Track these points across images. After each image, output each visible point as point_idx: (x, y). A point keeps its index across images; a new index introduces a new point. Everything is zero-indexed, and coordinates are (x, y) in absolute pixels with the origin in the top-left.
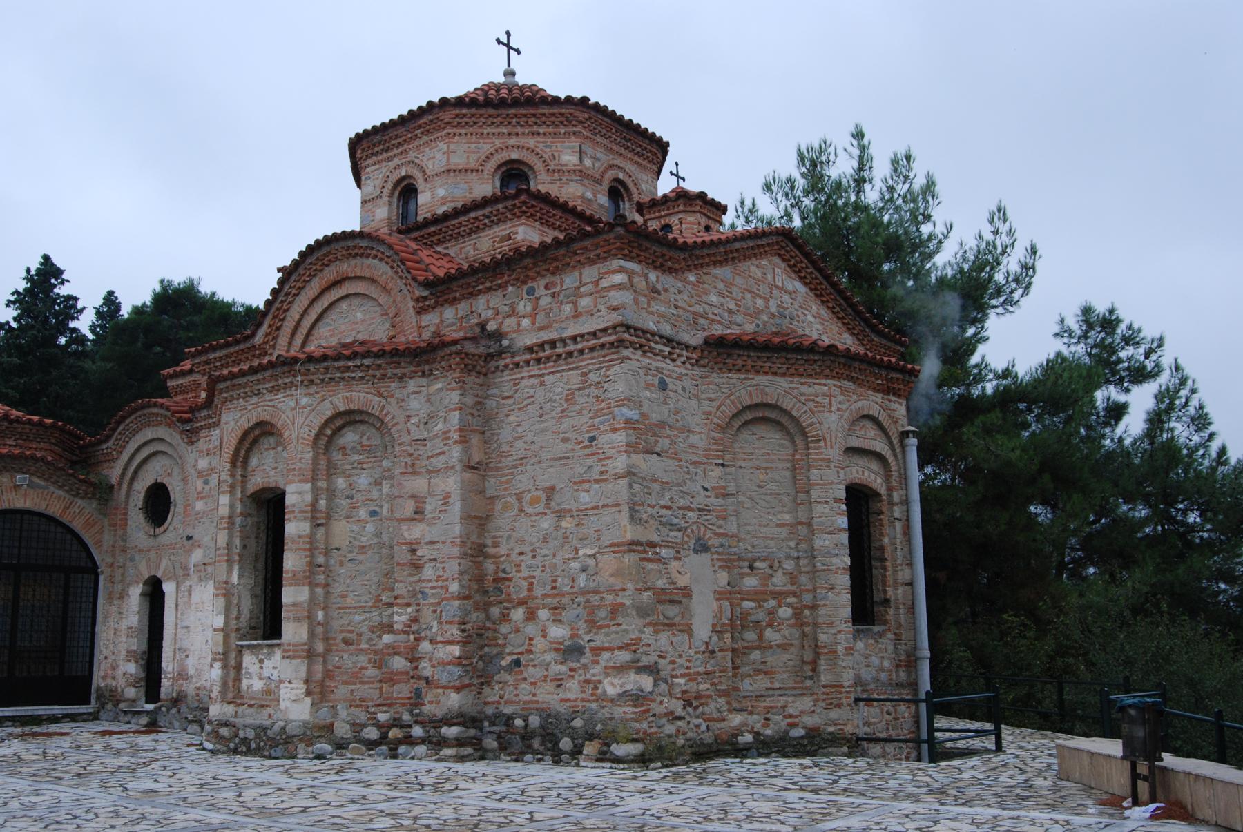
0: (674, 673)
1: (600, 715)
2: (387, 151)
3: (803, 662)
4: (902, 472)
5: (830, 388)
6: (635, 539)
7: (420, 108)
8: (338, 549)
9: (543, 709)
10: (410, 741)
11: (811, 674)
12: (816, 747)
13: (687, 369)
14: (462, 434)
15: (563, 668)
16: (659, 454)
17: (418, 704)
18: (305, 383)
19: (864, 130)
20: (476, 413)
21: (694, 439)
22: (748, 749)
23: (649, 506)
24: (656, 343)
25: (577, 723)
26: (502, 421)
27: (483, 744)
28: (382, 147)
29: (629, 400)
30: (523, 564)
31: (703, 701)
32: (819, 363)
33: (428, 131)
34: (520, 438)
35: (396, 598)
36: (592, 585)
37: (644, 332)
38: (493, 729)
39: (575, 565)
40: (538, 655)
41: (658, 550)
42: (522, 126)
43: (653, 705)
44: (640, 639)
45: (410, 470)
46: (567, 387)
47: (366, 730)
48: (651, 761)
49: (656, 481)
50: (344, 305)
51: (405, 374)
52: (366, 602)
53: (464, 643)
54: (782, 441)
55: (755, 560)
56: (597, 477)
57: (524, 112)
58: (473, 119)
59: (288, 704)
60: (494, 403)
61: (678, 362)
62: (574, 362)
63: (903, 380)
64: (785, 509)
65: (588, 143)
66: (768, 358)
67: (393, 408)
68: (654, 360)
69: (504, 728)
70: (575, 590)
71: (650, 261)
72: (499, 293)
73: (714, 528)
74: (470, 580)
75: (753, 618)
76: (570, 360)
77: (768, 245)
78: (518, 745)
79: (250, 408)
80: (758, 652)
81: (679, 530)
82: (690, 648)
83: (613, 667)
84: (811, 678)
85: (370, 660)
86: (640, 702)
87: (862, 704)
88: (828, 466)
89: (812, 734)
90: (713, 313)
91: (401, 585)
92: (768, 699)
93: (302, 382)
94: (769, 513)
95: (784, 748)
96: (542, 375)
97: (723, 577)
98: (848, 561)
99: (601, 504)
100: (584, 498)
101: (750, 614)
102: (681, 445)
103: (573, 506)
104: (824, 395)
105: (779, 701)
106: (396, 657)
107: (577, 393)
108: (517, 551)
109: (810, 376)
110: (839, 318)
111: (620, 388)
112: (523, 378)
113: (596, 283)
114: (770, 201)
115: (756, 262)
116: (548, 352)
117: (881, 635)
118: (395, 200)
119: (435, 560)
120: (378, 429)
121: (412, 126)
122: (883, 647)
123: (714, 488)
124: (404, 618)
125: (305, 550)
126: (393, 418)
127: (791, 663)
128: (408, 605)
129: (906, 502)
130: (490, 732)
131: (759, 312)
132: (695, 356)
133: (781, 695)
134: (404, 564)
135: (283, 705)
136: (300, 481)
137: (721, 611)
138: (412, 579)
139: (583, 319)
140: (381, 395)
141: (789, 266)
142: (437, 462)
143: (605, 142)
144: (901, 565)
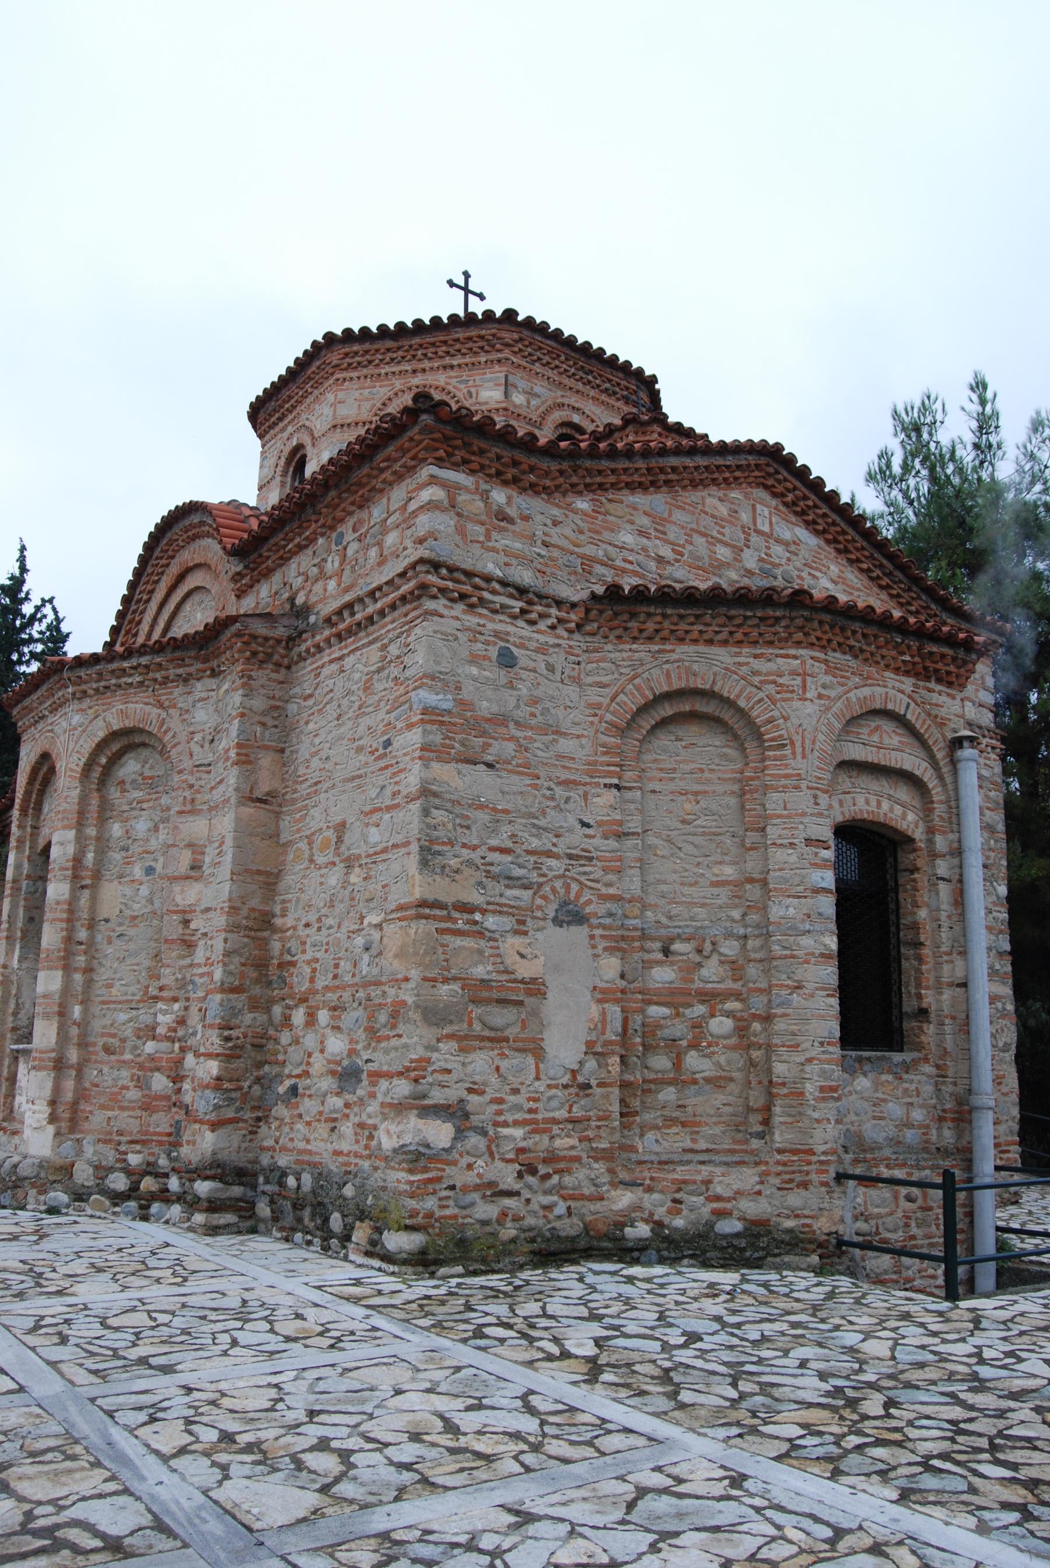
0: (501, 1118)
1: (371, 1182)
3: (749, 1109)
4: (953, 804)
5: (803, 662)
6: (430, 897)
7: (306, 352)
8: (107, 921)
10: (164, 1196)
11: (760, 1128)
12: (761, 1253)
13: (558, 637)
14: (244, 751)
15: (336, 1102)
16: (490, 766)
17: (177, 1145)
18: (78, 695)
19: (987, 380)
20: (270, 722)
21: (566, 745)
22: (642, 1250)
23: (464, 846)
24: (494, 592)
25: (349, 1191)
26: (302, 732)
27: (257, 1210)
29: (433, 678)
30: (308, 940)
31: (562, 1165)
32: (783, 624)
34: (316, 753)
35: (161, 989)
36: (375, 971)
37: (469, 574)
38: (268, 1188)
40: (316, 1080)
41: (478, 917)
42: (430, 359)
43: (449, 1170)
44: (428, 1061)
45: (189, 807)
46: (366, 670)
47: (112, 1177)
48: (439, 1263)
49: (481, 807)
51: (190, 674)
52: (134, 995)
53: (229, 1057)
54: (725, 750)
55: (672, 940)
56: (389, 803)
57: (432, 340)
58: (368, 357)
60: (295, 706)
61: (542, 625)
62: (376, 631)
63: (954, 659)
64: (727, 858)
65: (520, 373)
66: (697, 617)
67: (174, 723)
68: (493, 621)
69: (276, 1189)
70: (357, 979)
71: (493, 471)
72: (309, 551)
73: (598, 886)
74: (243, 965)
75: (666, 1033)
76: (371, 629)
77: (739, 467)
78: (289, 1220)
80: (672, 1089)
81: (526, 887)
82: (538, 1078)
83: (390, 1105)
84: (761, 1136)
85: (133, 1076)
86: (422, 1163)
87: (852, 1183)
88: (797, 788)
89: (756, 1230)
90: (625, 560)
91: (168, 970)
92: (679, 1168)
93: (74, 694)
94: (699, 864)
95: (704, 1252)
96: (341, 658)
97: (610, 967)
98: (832, 943)
99: (390, 844)
100: (375, 835)
101: (660, 1027)
102: (539, 753)
103: (361, 850)
104: (794, 673)
105: (699, 1172)
106: (156, 1074)
107: (376, 677)
108: (303, 922)
109: (770, 643)
110: (881, 587)
111: (419, 661)
112: (323, 666)
113: (404, 508)
114: (875, 494)
115: (721, 494)
117: (907, 1068)
118: (289, 479)
120: (161, 753)
122: (913, 1087)
123: (600, 824)
125: (61, 920)
126: (174, 736)
127: (728, 1109)
128: (175, 1000)
129: (958, 852)
130: (264, 1193)
131: (719, 566)
132: (573, 617)
133: (703, 1163)
134: (173, 941)
136: (64, 828)
137: (604, 1021)
138: (182, 963)
140: (161, 706)
141: (785, 504)
142: (217, 795)
143: (550, 373)
144: (950, 954)
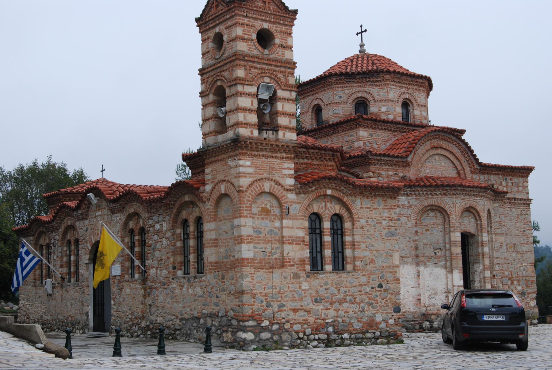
2: (399, 83)
33: (418, 85)
36: (527, 274)
39: (522, 268)
50: (437, 157)
79: (466, 200)
96: (511, 208)
100: (524, 248)
116: (513, 201)
119: (499, 264)
139: (520, 193)
142: (498, 231)
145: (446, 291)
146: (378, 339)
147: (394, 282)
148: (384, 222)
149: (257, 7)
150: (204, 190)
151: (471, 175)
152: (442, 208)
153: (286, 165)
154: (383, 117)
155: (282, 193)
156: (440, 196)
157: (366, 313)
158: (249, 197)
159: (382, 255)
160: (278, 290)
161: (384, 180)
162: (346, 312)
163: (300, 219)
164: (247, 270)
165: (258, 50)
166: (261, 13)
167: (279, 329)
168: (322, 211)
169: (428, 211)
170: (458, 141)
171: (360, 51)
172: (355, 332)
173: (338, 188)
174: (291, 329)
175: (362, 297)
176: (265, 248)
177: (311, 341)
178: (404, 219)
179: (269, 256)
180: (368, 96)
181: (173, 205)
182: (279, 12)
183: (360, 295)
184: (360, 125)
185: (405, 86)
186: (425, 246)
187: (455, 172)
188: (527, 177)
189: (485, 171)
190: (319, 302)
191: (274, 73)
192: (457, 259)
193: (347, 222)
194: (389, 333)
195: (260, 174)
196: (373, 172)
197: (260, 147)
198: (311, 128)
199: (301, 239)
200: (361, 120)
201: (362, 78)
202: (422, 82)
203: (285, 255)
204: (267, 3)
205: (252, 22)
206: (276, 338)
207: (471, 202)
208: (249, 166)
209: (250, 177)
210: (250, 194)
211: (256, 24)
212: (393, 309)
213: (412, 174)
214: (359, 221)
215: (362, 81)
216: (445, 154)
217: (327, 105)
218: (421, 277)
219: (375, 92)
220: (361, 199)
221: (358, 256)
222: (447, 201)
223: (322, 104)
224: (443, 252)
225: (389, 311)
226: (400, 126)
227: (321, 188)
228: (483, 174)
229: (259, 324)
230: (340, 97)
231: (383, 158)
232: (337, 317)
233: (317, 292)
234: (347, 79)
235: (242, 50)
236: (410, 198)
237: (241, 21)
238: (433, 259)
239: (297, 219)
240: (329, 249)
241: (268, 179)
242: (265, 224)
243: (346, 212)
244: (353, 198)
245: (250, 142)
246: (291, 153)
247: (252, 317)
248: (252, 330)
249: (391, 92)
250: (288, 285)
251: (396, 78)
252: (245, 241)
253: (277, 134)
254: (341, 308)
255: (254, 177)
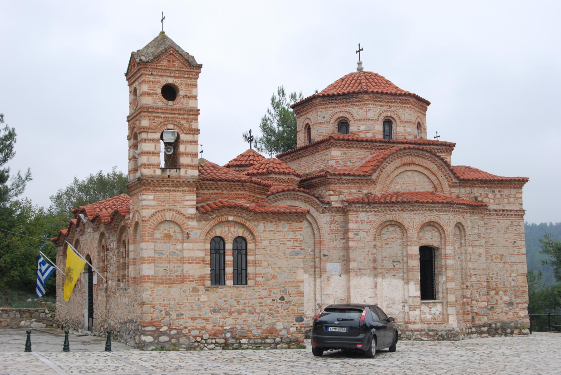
9: (502, 321)
10: (472, 333)
15: (507, 309)
28: (379, 99)
33: (402, 102)
36: (516, 285)
39: (510, 279)
50: (409, 173)
59: (453, 322)
96: (498, 219)
103: (509, 261)
108: (492, 273)
116: (501, 212)
121: (396, 98)
124: (469, 293)
135: (450, 322)
139: (511, 205)
145: (403, 301)
146: (278, 344)
147: (297, 295)
148: (289, 244)
149: (162, 66)
150: (129, 218)
151: (449, 189)
152: (400, 223)
153: (188, 197)
154: (362, 135)
155: (183, 221)
156: (398, 212)
157: (266, 322)
158: (151, 225)
159: (285, 272)
160: (177, 301)
161: (345, 197)
162: (245, 321)
163: (200, 242)
164: (148, 285)
165: (163, 102)
166: (166, 71)
167: (178, 333)
168: (225, 235)
169: (387, 226)
170: (433, 157)
171: (358, 69)
172: (254, 338)
173: (239, 214)
174: (189, 334)
175: (263, 308)
176: (167, 267)
177: (208, 344)
178: (362, 234)
179: (170, 273)
180: (348, 116)
181: (117, 228)
182: (183, 68)
183: (260, 306)
184: (332, 145)
185: (387, 104)
186: (384, 259)
187: (432, 186)
188: (522, 188)
189: (466, 185)
190: (217, 312)
191: (178, 120)
192: (413, 271)
193: (250, 243)
194: (290, 339)
195: (162, 206)
196: (333, 191)
197: (162, 183)
198: (304, 146)
199: (201, 259)
200: (332, 140)
201: (343, 99)
202: (406, 100)
203: (185, 272)
204: (171, 61)
205: (158, 79)
206: (174, 341)
207: (432, 217)
208: (152, 200)
209: (152, 208)
210: (152, 222)
211: (160, 80)
212: (295, 318)
213: (377, 191)
214: (261, 243)
215: (343, 102)
216: (418, 170)
217: (314, 124)
218: (378, 287)
219: (355, 112)
220: (264, 223)
221: (259, 272)
222: (405, 216)
223: (310, 124)
224: (401, 265)
225: (290, 321)
226: (377, 144)
227: (223, 216)
228: (464, 188)
229: (158, 330)
230: (324, 117)
231: (344, 178)
232: (235, 324)
233: (216, 304)
234: (329, 100)
235: (146, 103)
236: (369, 214)
237: (147, 79)
238: (392, 271)
239: (197, 242)
240: (230, 267)
241: (170, 210)
242: (166, 247)
243: (249, 234)
244: (256, 223)
245: (152, 181)
246: (194, 187)
247: (151, 324)
248: (151, 334)
249: (370, 111)
250: (186, 298)
251: (376, 97)
252: (147, 261)
253: (180, 172)
254: (240, 317)
255: (156, 209)
